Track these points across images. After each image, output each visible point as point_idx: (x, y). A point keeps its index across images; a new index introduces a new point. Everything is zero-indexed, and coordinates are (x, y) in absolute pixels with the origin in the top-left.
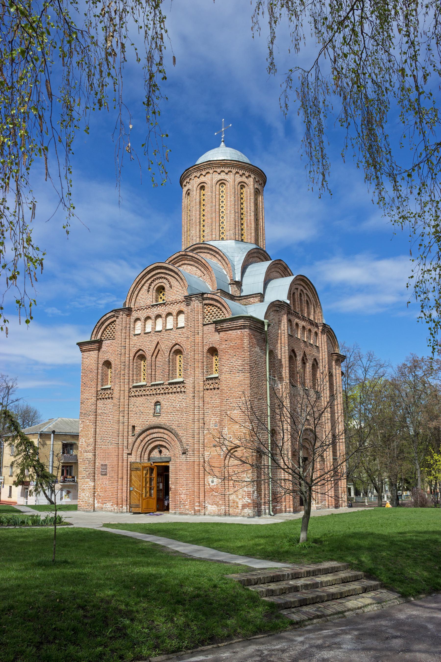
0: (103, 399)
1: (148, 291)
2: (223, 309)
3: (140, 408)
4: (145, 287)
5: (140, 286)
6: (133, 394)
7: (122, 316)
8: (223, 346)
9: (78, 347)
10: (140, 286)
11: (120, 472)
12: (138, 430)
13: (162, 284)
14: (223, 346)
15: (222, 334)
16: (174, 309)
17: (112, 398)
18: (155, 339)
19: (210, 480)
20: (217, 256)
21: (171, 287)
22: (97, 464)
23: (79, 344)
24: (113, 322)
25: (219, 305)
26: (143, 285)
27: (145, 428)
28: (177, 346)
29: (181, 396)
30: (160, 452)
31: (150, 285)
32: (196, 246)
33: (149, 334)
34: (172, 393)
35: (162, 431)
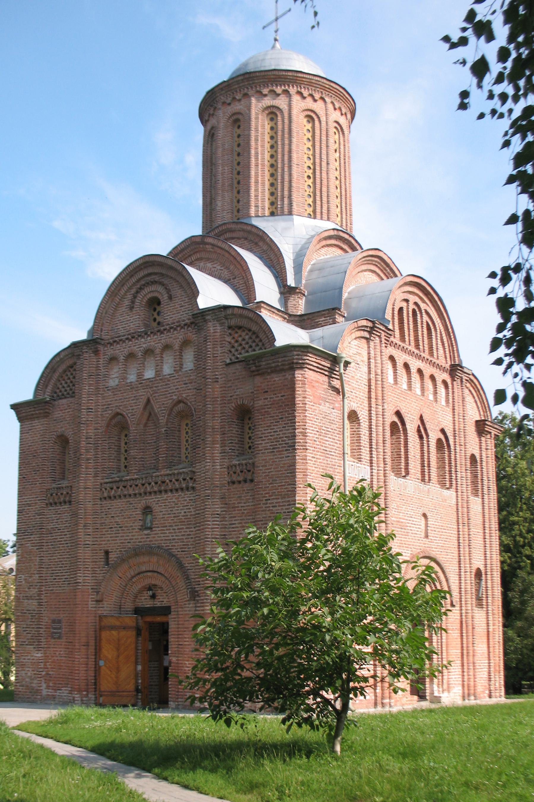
0: (56, 503)
1: (131, 308)
2: (261, 335)
3: (117, 519)
4: (127, 303)
5: (117, 300)
8: (261, 403)
9: (13, 413)
13: (156, 294)
14: (261, 403)
15: (258, 380)
20: (261, 244)
23: (15, 407)
25: (254, 328)
26: (123, 297)
28: (181, 405)
29: (188, 495)
30: (153, 597)
31: (135, 297)
32: (224, 227)
34: (171, 491)
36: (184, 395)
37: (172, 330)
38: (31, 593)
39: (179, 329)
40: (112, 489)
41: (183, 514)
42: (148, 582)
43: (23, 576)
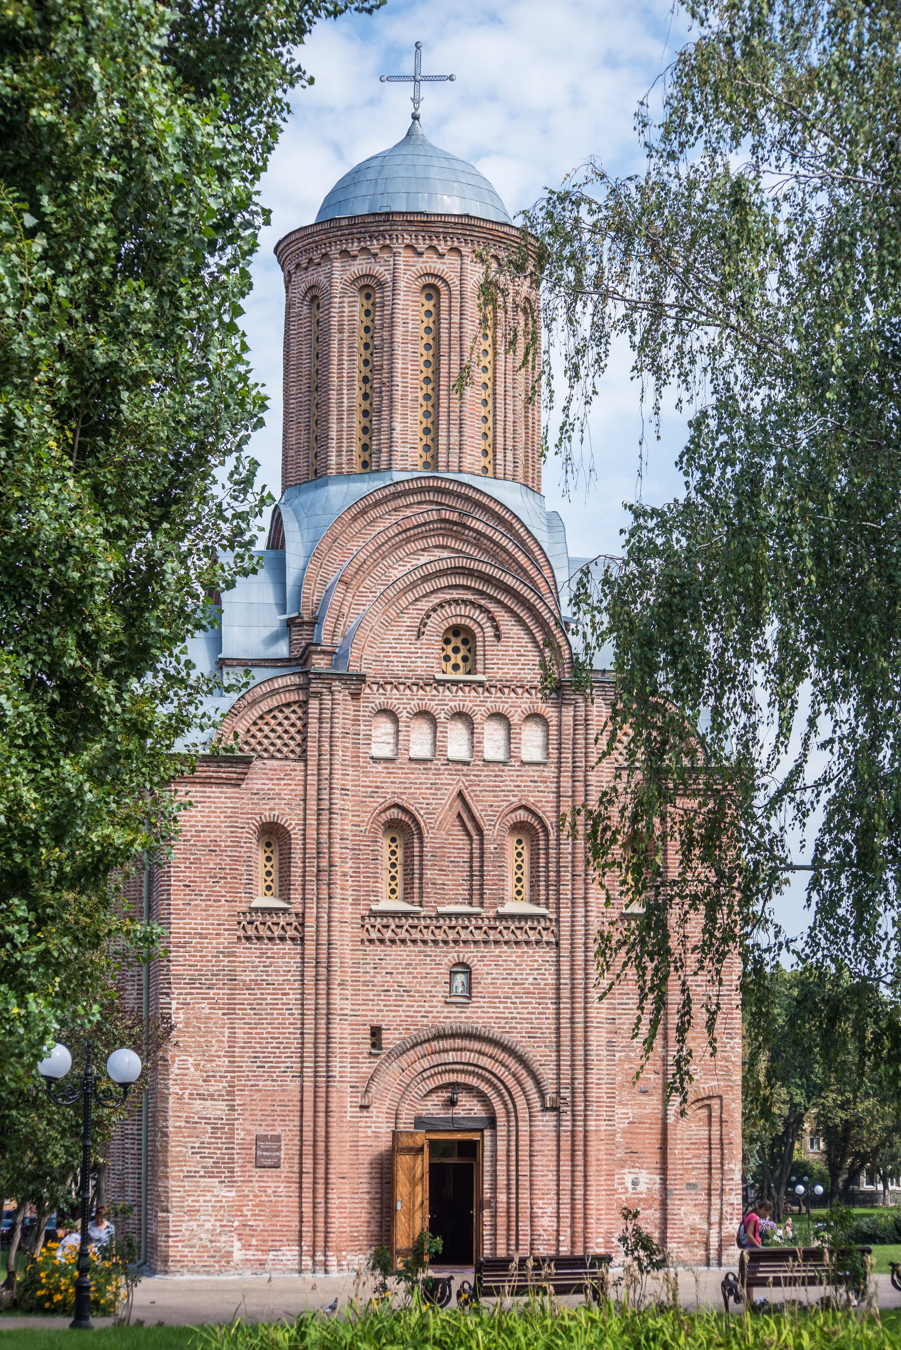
1: (420, 634)
6: (374, 935)
7: (342, 695)
13: (468, 622)
17: (293, 939)
18: (451, 784)
19: (628, 1179)
21: (498, 637)
22: (240, 1134)
24: (288, 705)
27: (424, 1035)
33: (429, 765)
36: (532, 800)
37: (506, 690)
38: (211, 1089)
39: (520, 691)
40: (386, 927)
41: (531, 980)
43: (191, 1060)
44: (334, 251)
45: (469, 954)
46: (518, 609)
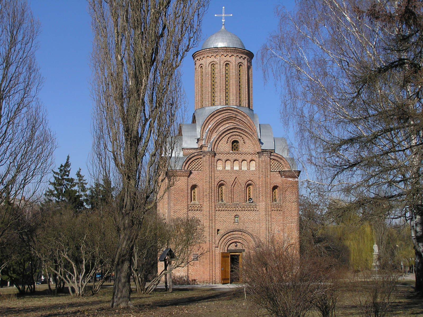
3: (223, 219)
6: (217, 209)
10: (221, 138)
11: (211, 259)
12: (222, 232)
13: (237, 139)
16: (249, 158)
24: (198, 159)
28: (250, 181)
35: (240, 233)
42: (235, 240)
44: (206, 56)
45: (238, 213)
46: (249, 136)
